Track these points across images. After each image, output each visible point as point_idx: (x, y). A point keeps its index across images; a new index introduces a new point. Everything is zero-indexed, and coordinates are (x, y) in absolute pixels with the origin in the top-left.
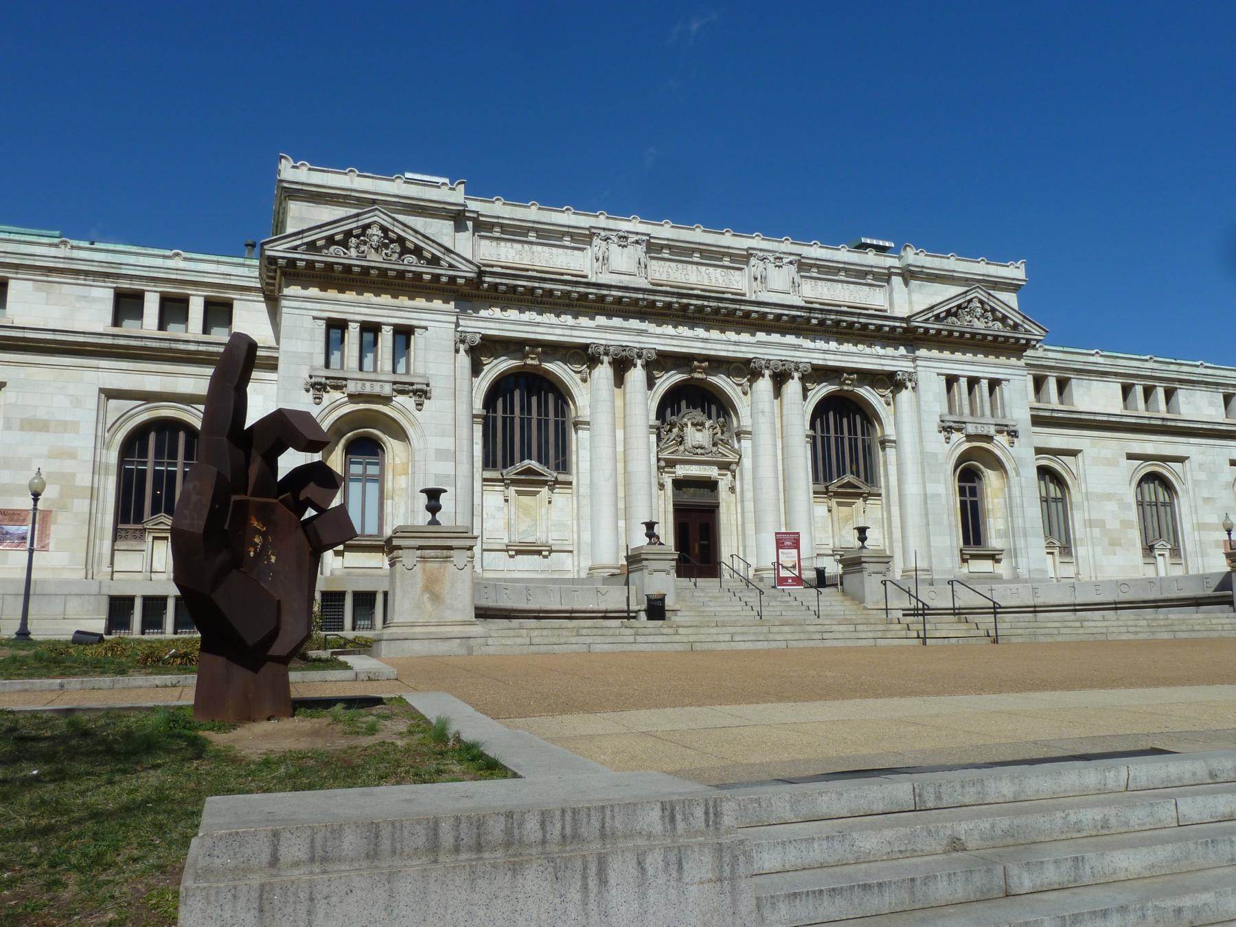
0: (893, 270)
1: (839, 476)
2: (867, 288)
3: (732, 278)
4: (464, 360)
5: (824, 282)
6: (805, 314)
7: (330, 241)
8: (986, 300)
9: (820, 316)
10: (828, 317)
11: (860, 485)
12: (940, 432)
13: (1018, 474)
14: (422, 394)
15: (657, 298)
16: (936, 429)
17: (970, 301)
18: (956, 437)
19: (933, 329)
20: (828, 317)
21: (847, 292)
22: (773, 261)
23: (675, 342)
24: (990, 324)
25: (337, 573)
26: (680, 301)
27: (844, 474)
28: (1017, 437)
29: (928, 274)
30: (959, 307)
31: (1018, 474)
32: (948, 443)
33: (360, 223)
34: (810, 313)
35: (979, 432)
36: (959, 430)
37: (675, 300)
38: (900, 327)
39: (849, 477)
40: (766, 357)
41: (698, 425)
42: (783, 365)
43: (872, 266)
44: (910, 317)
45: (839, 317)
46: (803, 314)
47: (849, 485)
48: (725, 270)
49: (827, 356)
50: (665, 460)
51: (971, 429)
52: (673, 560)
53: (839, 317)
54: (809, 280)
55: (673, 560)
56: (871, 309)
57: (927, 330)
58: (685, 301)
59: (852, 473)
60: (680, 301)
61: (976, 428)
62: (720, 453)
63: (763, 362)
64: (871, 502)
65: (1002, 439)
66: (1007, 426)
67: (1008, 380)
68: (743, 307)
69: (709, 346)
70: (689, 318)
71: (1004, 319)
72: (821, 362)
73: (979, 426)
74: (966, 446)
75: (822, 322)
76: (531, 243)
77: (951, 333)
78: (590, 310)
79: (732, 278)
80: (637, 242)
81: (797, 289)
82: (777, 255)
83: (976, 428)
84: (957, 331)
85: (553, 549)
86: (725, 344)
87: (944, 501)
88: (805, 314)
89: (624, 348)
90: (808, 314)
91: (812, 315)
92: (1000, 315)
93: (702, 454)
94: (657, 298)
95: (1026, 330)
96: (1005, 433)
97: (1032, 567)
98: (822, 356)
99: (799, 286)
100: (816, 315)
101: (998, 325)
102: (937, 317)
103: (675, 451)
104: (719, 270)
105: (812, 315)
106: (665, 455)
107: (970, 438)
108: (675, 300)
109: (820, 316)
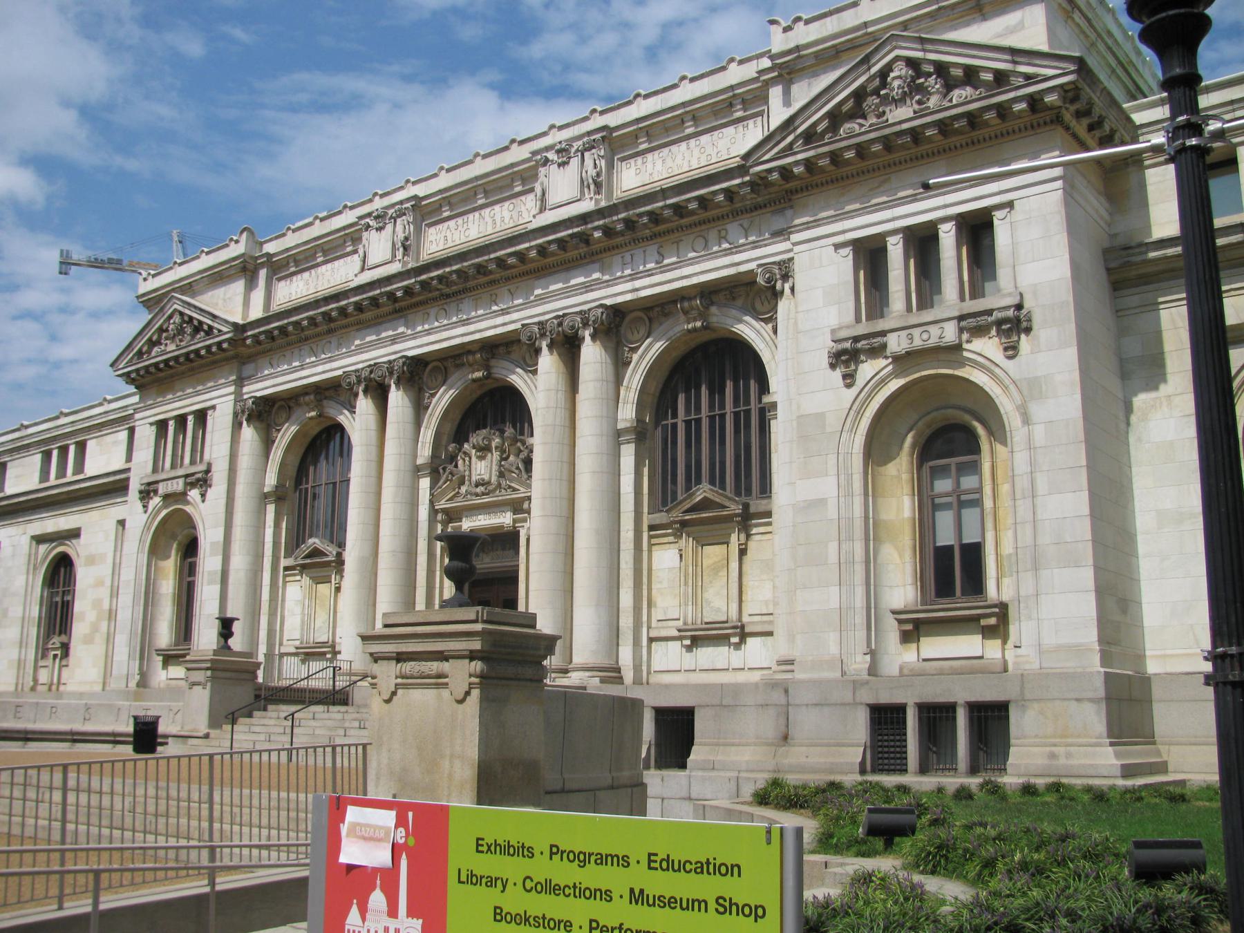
1: (688, 488)
2: (730, 130)
3: (522, 206)
4: (249, 433)
6: (579, 229)
7: (152, 343)
8: (919, 55)
9: (601, 222)
11: (727, 503)
12: (833, 366)
13: (1026, 420)
14: (202, 482)
15: (395, 286)
16: (825, 361)
17: (888, 69)
18: (868, 369)
19: (797, 163)
20: (615, 218)
21: (696, 152)
22: (555, 158)
23: (432, 338)
24: (933, 102)
25: (162, 685)
26: (419, 279)
27: (699, 481)
28: (1028, 330)
29: (816, 55)
30: (859, 95)
31: (1026, 420)
32: (849, 386)
33: (165, 316)
34: (586, 223)
35: (918, 343)
36: (877, 351)
37: (413, 280)
38: (743, 184)
39: (704, 491)
40: (536, 320)
41: (484, 450)
42: (560, 324)
43: (732, 88)
44: (746, 156)
45: (631, 212)
46: (576, 230)
47: (705, 504)
48: (514, 201)
49: (638, 284)
50: (444, 511)
51: (896, 343)
52: (207, 669)
54: (632, 161)
55: (207, 669)
57: (785, 172)
58: (424, 277)
59: (712, 482)
60: (419, 279)
61: (911, 338)
62: (510, 487)
63: (536, 329)
64: (762, 529)
65: (988, 347)
66: (989, 312)
67: (1010, 205)
68: (492, 256)
69: (472, 328)
70: (448, 296)
71: (970, 76)
72: (629, 297)
73: (916, 332)
74: (895, 384)
75: (608, 232)
76: (318, 265)
77: (861, 150)
78: (351, 329)
79: (523, 208)
80: (401, 214)
82: (558, 147)
83: (911, 338)
84: (848, 148)
85: (747, 630)
86: (491, 318)
87: (832, 512)
88: (579, 229)
89: (373, 367)
92: (958, 72)
93: (483, 494)
94: (395, 286)
95: (1028, 77)
96: (994, 332)
97: (1049, 640)
98: (629, 286)
100: (596, 223)
101: (967, 92)
102: (810, 137)
103: (454, 496)
104: (506, 204)
105: (590, 226)
106: (443, 504)
107: (903, 361)
108: (413, 280)
109: (601, 222)
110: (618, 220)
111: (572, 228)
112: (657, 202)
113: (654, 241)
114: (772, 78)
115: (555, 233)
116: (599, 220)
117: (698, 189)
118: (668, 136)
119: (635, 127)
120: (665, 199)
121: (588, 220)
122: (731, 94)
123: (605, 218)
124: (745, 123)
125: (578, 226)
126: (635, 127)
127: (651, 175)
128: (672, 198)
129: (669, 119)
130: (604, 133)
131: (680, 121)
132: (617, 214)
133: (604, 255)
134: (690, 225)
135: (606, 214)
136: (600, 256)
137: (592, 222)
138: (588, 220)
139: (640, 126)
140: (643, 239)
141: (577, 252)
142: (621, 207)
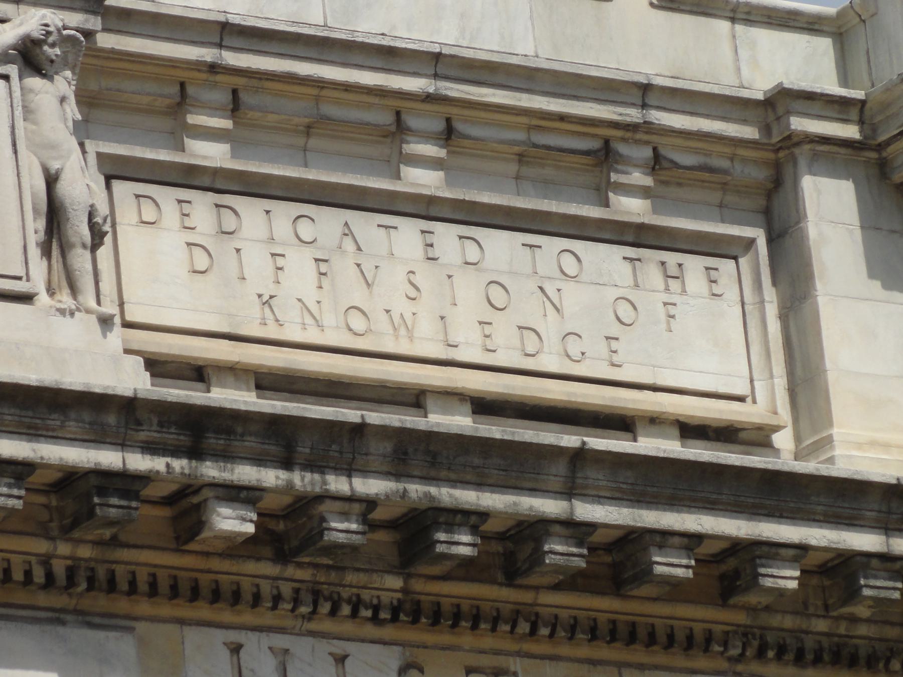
0: (801, 124)
5: (284, 211)
10: (338, 484)
20: (338, 484)
34: (195, 453)
45: (416, 490)
46: (139, 462)
53: (416, 490)
54: (166, 196)
56: (655, 421)
81: (81, 259)
88: (156, 464)
90: (179, 464)
91: (211, 471)
99: (97, 236)
105: (211, 471)
110: (351, 499)
111: (123, 445)
112: (534, 491)
113: (388, 632)
114: (825, 140)
115: (33, 433)
116: (259, 461)
117: (711, 506)
118: (304, 157)
119: (207, 54)
120: (569, 492)
121: (213, 441)
122: (633, 115)
123: (287, 464)
124: (672, 258)
125: (150, 448)
126: (207, 54)
127: (267, 302)
128: (599, 499)
129: (347, 87)
130: (94, 23)
131: (385, 118)
132: (349, 471)
133: (144, 607)
134: (573, 629)
135: (303, 450)
136: (122, 605)
137: (226, 456)
138: (213, 441)
139: (232, 59)
140: (356, 605)
141: (41, 546)
142: (380, 448)
